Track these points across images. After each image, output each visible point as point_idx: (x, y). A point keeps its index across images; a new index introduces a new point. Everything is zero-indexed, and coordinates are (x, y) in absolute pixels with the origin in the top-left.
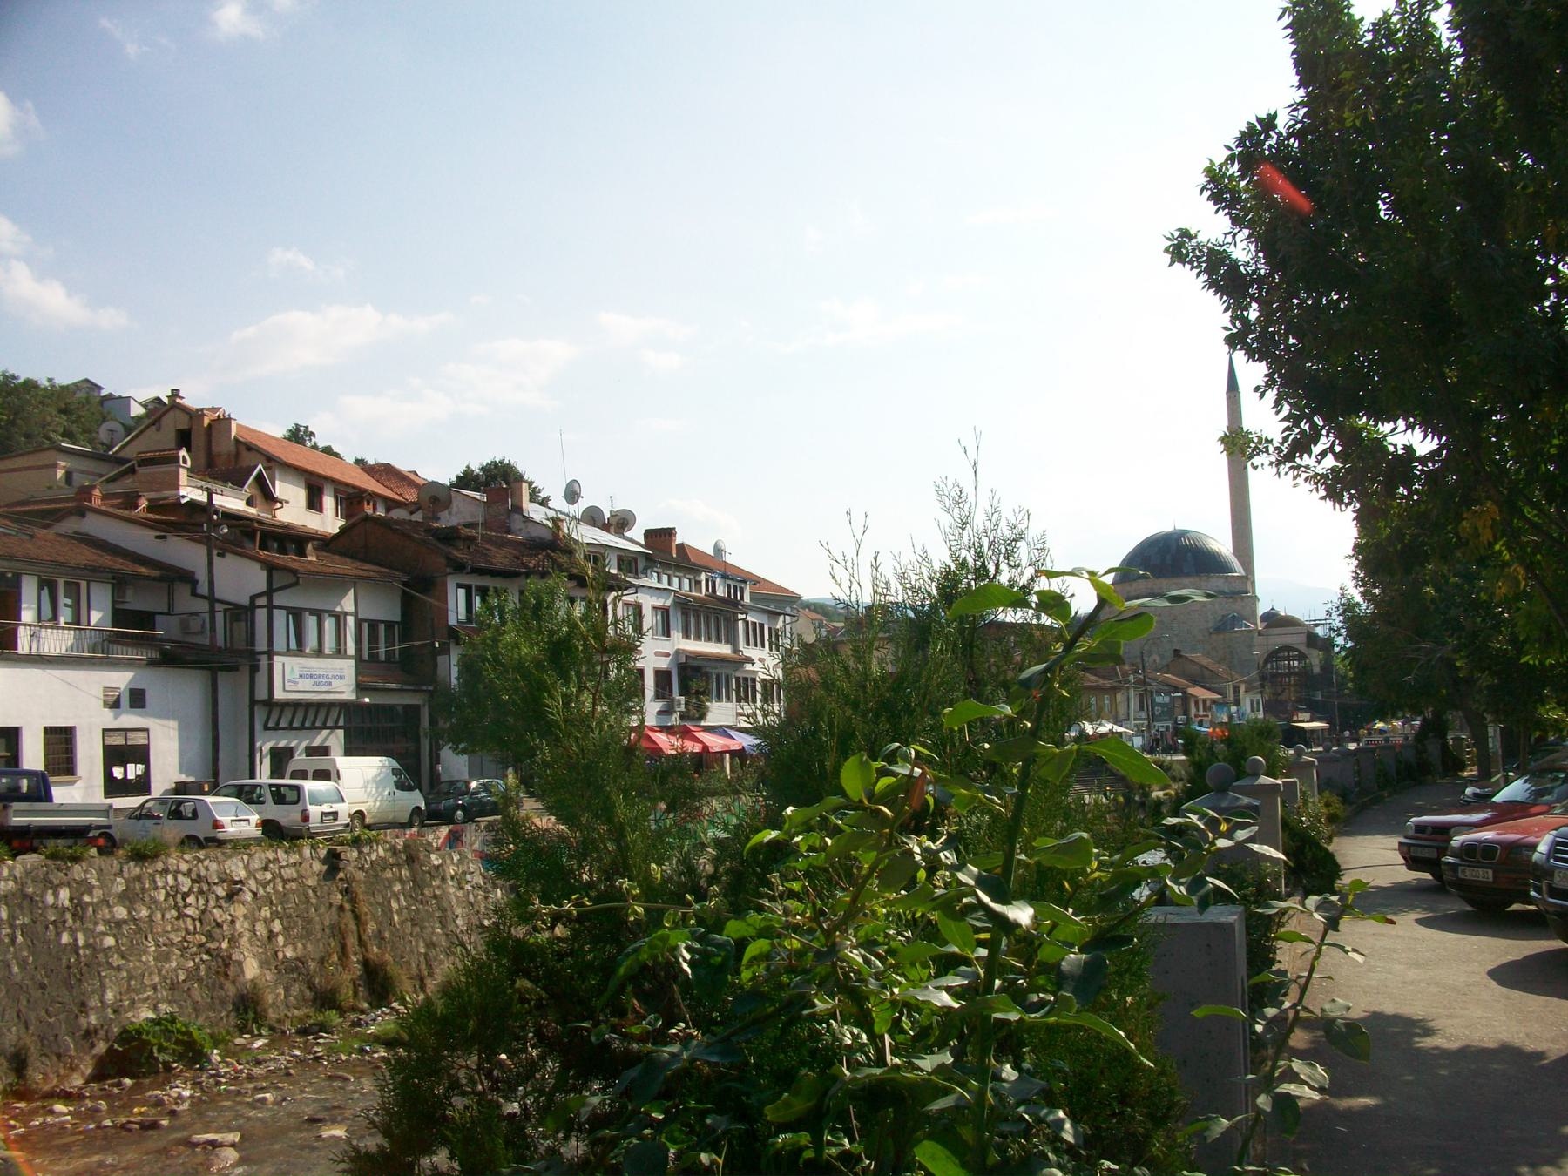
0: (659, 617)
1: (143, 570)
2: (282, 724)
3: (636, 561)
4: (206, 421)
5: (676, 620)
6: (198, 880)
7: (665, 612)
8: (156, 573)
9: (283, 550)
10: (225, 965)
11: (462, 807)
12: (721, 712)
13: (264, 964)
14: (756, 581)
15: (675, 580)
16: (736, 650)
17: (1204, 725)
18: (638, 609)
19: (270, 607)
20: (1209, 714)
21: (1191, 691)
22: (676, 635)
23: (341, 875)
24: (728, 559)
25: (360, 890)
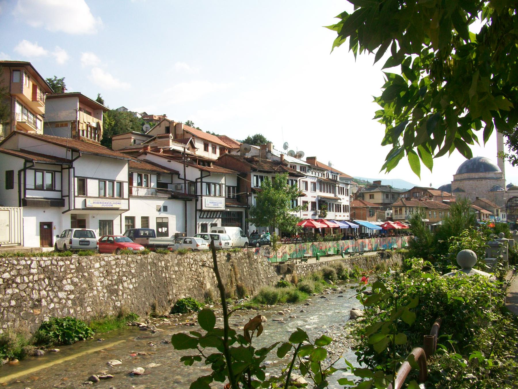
0: (313, 185)
1: (166, 171)
2: (204, 217)
3: (305, 167)
4: (174, 124)
5: (318, 186)
6: (195, 260)
7: (315, 183)
8: (169, 172)
9: (204, 165)
10: (202, 284)
11: (258, 242)
12: (330, 215)
13: (211, 285)
14: (341, 174)
15: (317, 174)
16: (335, 196)
18: (306, 183)
19: (202, 182)
21: (482, 211)
22: (318, 191)
23: (231, 261)
24: (333, 167)
25: (236, 265)
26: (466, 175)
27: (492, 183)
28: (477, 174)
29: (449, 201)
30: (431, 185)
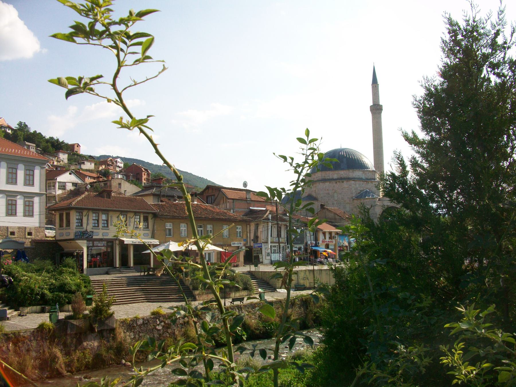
17: (330, 247)
20: (334, 241)
26: (319, 175)
27: (358, 186)
28: (336, 172)
29: (264, 209)
30: (245, 185)
